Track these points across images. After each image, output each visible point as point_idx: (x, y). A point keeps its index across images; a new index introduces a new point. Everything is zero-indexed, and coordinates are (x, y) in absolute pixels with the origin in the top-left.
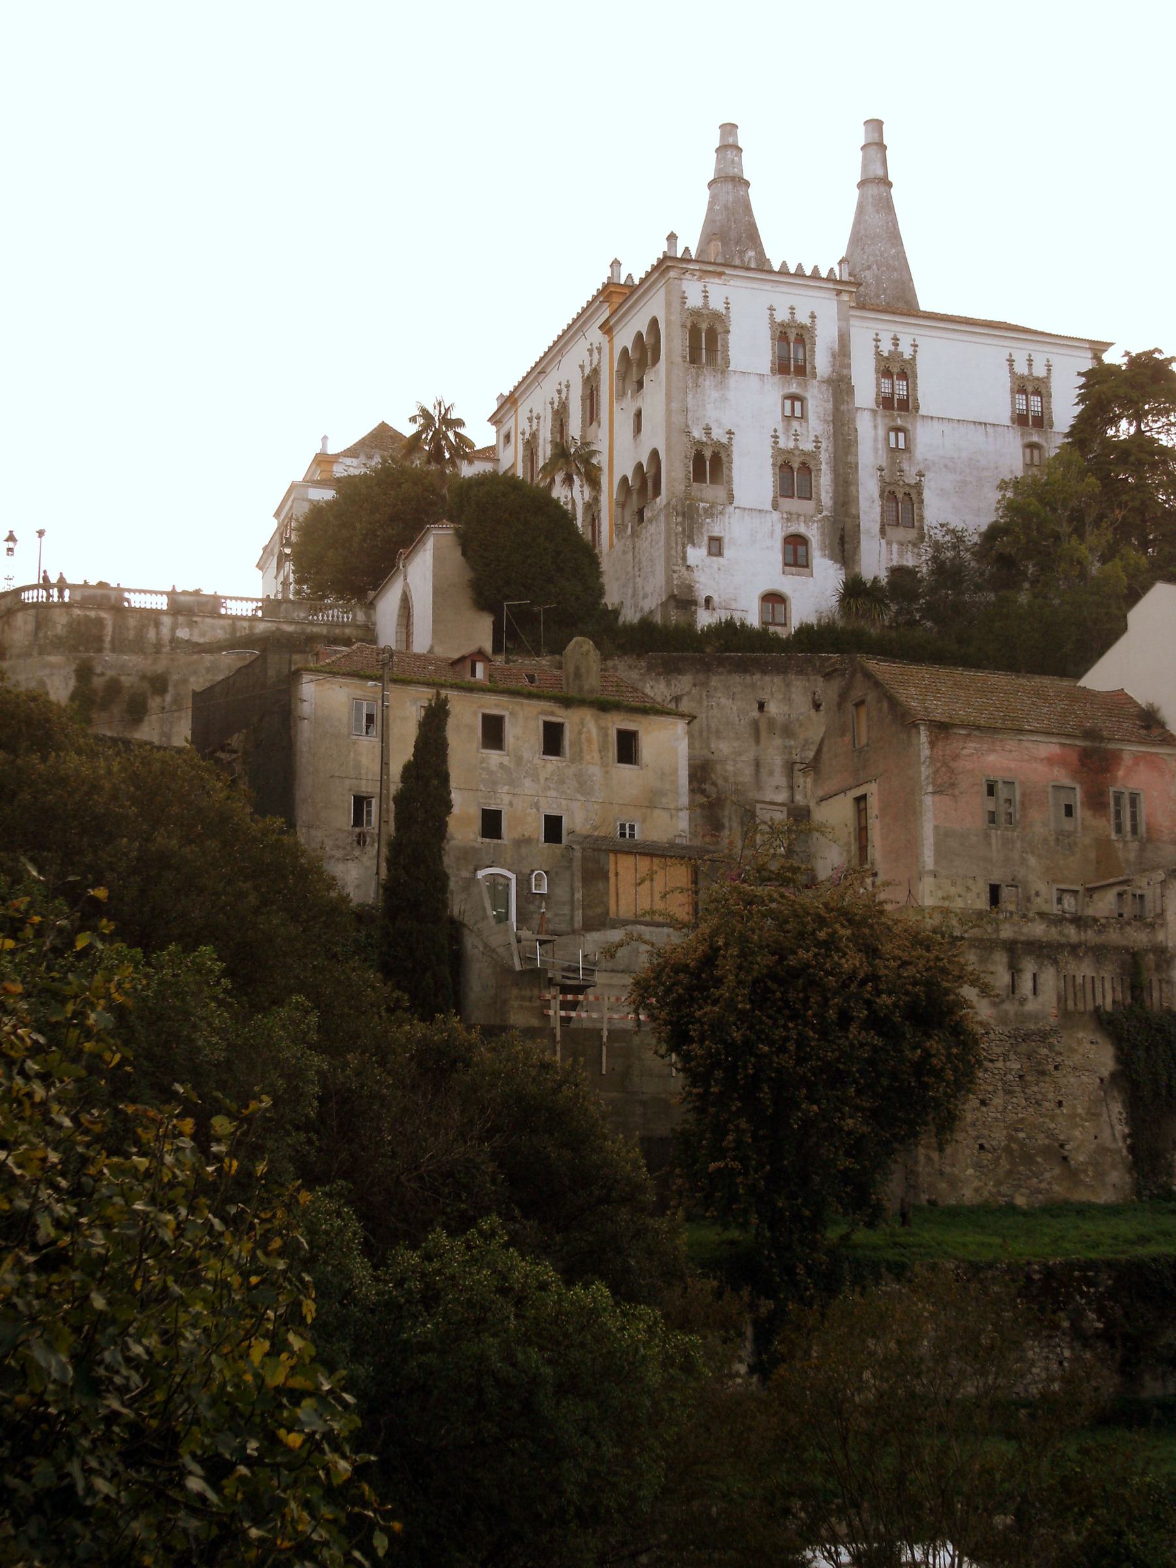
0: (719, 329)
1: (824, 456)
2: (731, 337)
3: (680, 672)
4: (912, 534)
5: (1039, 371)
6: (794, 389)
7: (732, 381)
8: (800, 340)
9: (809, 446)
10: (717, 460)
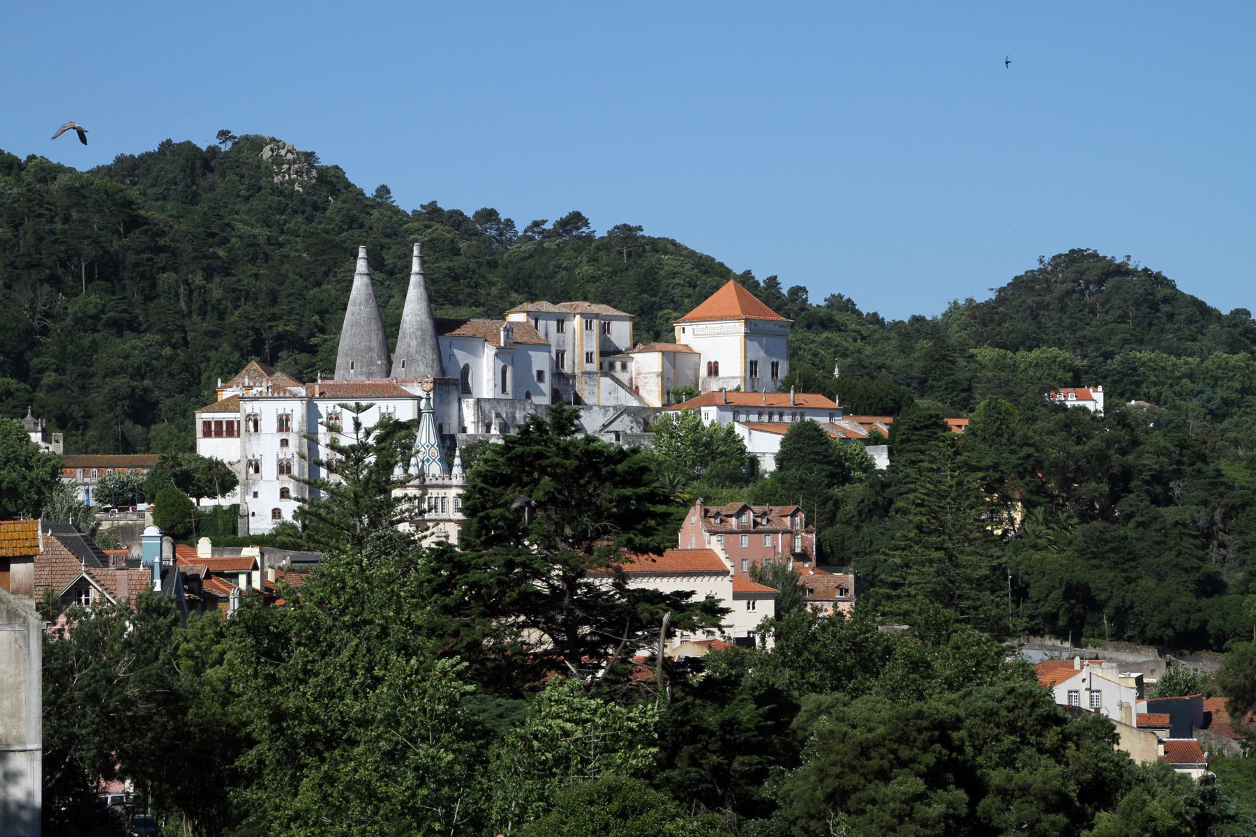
7: (262, 437)
9: (289, 456)
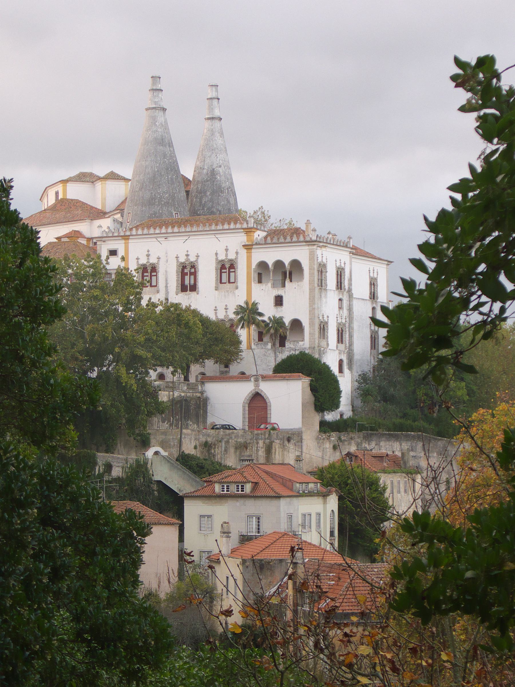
0: (324, 270)
1: (347, 325)
2: (328, 274)
5: (375, 276)
6: (341, 297)
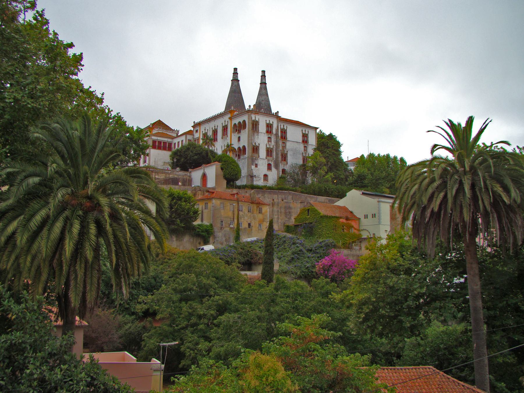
3: (259, 193)
4: (285, 163)
5: (307, 133)
6: (270, 136)
7: (260, 134)
8: (271, 127)
10: (256, 149)
